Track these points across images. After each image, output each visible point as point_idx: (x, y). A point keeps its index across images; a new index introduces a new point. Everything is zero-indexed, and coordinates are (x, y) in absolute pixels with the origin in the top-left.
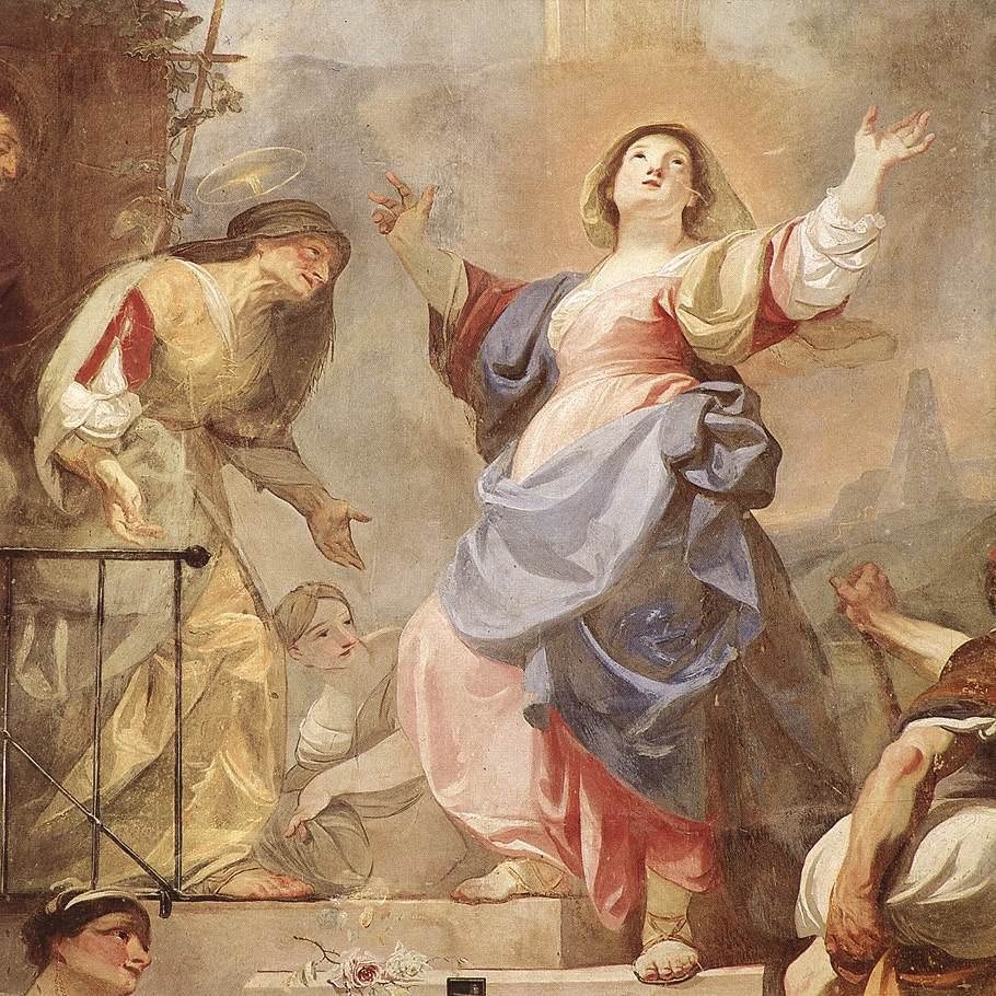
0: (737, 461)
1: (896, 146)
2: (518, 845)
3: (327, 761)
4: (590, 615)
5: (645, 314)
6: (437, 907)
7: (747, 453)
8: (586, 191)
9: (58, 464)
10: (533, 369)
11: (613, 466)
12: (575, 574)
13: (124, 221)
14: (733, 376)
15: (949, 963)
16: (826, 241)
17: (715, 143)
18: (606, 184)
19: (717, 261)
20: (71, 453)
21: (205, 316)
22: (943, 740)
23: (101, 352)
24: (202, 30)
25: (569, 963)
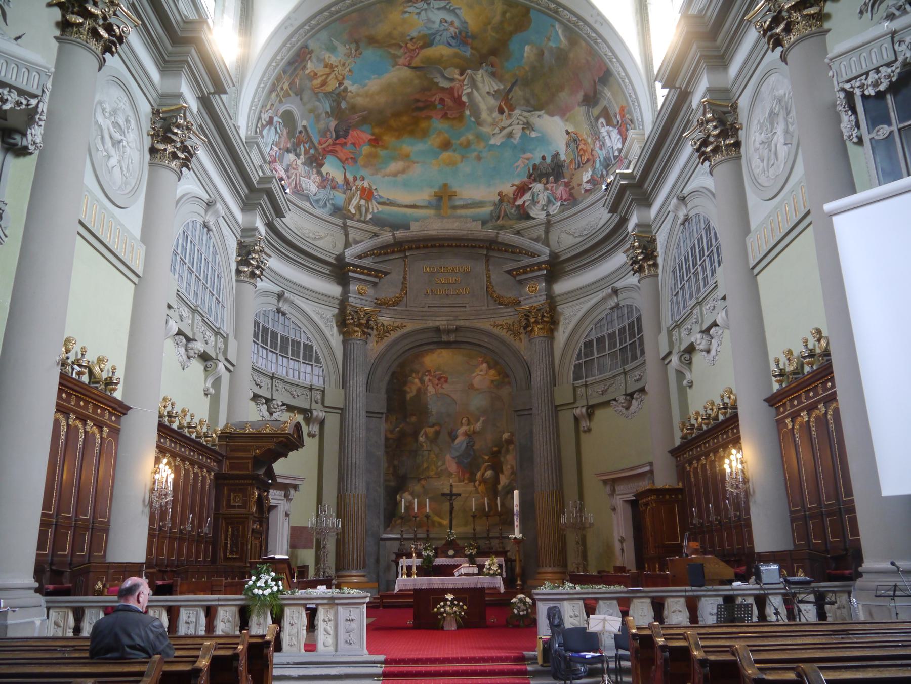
0: (471, 443)
1: (483, 419)
3: (440, 467)
8: (460, 421)
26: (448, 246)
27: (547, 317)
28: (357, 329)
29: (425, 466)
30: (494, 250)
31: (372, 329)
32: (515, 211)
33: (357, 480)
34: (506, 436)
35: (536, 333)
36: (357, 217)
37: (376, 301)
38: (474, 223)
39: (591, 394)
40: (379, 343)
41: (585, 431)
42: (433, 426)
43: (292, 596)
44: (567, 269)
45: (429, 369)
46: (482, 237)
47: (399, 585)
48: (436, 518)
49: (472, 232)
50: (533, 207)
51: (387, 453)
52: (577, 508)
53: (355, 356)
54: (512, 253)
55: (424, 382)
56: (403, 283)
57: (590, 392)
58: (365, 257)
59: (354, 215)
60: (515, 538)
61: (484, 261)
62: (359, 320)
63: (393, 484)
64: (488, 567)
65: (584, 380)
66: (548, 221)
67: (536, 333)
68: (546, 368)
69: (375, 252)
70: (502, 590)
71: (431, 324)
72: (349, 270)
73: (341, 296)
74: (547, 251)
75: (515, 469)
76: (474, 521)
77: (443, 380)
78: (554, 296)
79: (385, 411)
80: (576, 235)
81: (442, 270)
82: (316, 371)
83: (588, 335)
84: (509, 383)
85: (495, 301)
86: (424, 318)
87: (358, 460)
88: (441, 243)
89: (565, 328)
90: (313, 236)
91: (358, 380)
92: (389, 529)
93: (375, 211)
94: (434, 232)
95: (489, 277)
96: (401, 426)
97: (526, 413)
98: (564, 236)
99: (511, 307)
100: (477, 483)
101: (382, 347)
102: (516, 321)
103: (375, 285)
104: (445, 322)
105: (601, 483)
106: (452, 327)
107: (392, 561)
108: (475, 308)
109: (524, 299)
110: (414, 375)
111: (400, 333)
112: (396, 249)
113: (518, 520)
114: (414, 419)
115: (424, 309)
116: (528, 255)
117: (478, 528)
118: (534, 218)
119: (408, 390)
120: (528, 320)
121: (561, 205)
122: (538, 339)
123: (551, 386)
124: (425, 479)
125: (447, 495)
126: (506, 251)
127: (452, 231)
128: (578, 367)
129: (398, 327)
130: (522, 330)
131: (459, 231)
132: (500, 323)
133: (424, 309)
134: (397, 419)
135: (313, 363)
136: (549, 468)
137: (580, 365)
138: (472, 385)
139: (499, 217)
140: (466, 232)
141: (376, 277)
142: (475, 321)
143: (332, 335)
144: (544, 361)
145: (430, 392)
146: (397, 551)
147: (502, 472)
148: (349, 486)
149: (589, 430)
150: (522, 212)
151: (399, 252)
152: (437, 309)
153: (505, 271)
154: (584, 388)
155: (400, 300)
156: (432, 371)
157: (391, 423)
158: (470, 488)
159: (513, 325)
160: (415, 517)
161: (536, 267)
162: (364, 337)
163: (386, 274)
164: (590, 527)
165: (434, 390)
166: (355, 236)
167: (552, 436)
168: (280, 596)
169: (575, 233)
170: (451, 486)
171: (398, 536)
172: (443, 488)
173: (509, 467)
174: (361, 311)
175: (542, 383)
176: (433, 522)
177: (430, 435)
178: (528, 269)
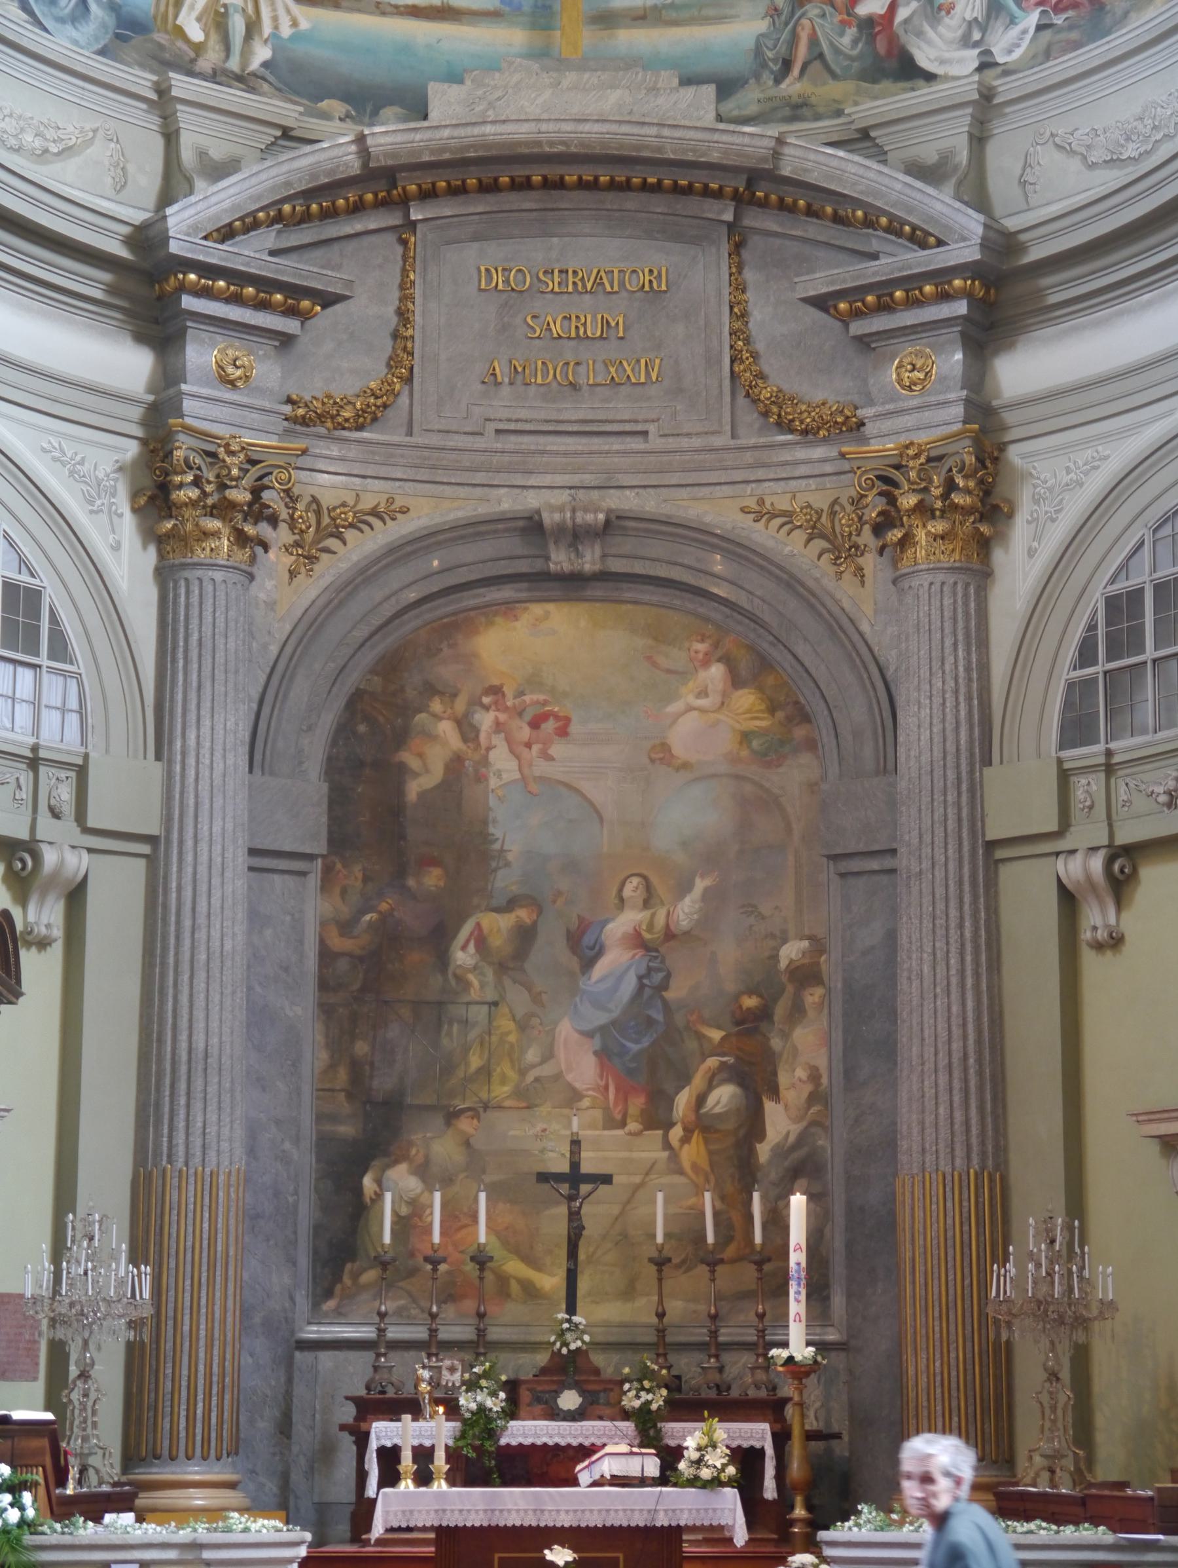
0: (658, 977)
2: (590, 1093)
3: (533, 1066)
4: (613, 1023)
5: (631, 931)
6: (566, 1111)
7: (661, 975)
9: (455, 976)
10: (597, 948)
11: (620, 979)
12: (610, 1011)
13: (475, 901)
14: (657, 951)
15: (717, 1131)
16: (687, 910)
17: (655, 880)
18: (621, 890)
19: (653, 915)
20: (458, 972)
21: (499, 930)
22: (717, 1064)
23: (467, 942)
24: (500, 842)
25: (605, 1128)
26: (582, 185)
27: (968, 492)
28: (213, 524)
29: (475, 1061)
30: (763, 204)
31: (274, 521)
32: (855, 42)
33: (213, 1117)
34: (792, 951)
35: (921, 554)
36: (205, 64)
37: (287, 409)
38: (689, 92)
39: (1127, 803)
40: (301, 578)
41: (1099, 947)
42: (510, 905)
43: (67, 1539)
44: (1053, 299)
45: (496, 682)
46: (715, 157)
47: (386, 1513)
48: (515, 1267)
49: (678, 133)
50: (927, 28)
51: (326, 1010)
52: (1053, 1241)
53: (207, 630)
54: (837, 219)
55: (477, 731)
56: (395, 335)
57: (1122, 793)
58: (247, 230)
59: (199, 48)
60: (791, 1359)
61: (725, 248)
62: (222, 487)
63: (346, 1130)
64: (695, 1455)
65: (1100, 747)
66: (987, 96)
67: (921, 554)
68: (956, 692)
69: (287, 208)
70: (741, 1537)
71: (507, 502)
72: (182, 288)
73: (150, 390)
74: (973, 224)
75: (825, 1081)
76: (660, 1280)
77: (550, 726)
78: (995, 403)
79: (319, 846)
80: (1095, 156)
81: (554, 284)
82: (53, 690)
83: (1124, 566)
84: (811, 745)
85: (766, 414)
86: (480, 478)
87: (214, 1041)
88: (553, 172)
89: (1038, 537)
90: (38, 143)
91: (219, 728)
92: (330, 1304)
93: (286, 31)
94: (525, 128)
95: (740, 315)
96: (384, 906)
97: (875, 865)
98: (1048, 157)
99: (825, 440)
100: (676, 1133)
101: (313, 593)
102: (844, 501)
103: (285, 341)
104: (563, 497)
105: (1155, 1148)
106: (589, 517)
107: (343, 1427)
108: (685, 443)
109: (877, 416)
110: (436, 706)
111: (381, 536)
112: (369, 197)
113: (803, 1297)
114: (433, 879)
115: (479, 443)
116: (899, 234)
117: (676, 1308)
118: (930, 77)
119: (413, 763)
120: (892, 500)
121: (1040, 28)
122: (925, 579)
123: (971, 765)
124: (474, 1113)
125: (559, 1178)
126: (811, 212)
127: (597, 128)
128: (1079, 692)
129: (374, 513)
130: (867, 537)
131: (625, 129)
132: (783, 504)
133: (479, 443)
134: (366, 879)
135: (43, 660)
136: (957, 1084)
137: (1091, 682)
138: (665, 747)
139: (787, 65)
140: (653, 131)
141: (291, 312)
142: (684, 493)
143: (116, 547)
144: (947, 667)
145: (499, 774)
146: (362, 1392)
147: (775, 1093)
148: (180, 1138)
149: (1115, 941)
150: (881, 46)
151: (382, 204)
152: (527, 442)
153: (809, 301)
154: (1102, 775)
155: (385, 406)
156: (509, 691)
157: (344, 892)
158: (650, 1149)
159: (833, 514)
160: (435, 1262)
161: (928, 289)
162: (242, 555)
163: (328, 300)
164: (1102, 1316)
165: (513, 764)
166: (203, 141)
167: (969, 958)
168: (28, 1539)
169: (1089, 147)
170: (576, 1144)
171: (366, 1332)
172: (543, 1151)
173: (801, 1073)
174: (232, 453)
175: (937, 753)
176: (503, 1280)
177: (496, 942)
178: (898, 294)
